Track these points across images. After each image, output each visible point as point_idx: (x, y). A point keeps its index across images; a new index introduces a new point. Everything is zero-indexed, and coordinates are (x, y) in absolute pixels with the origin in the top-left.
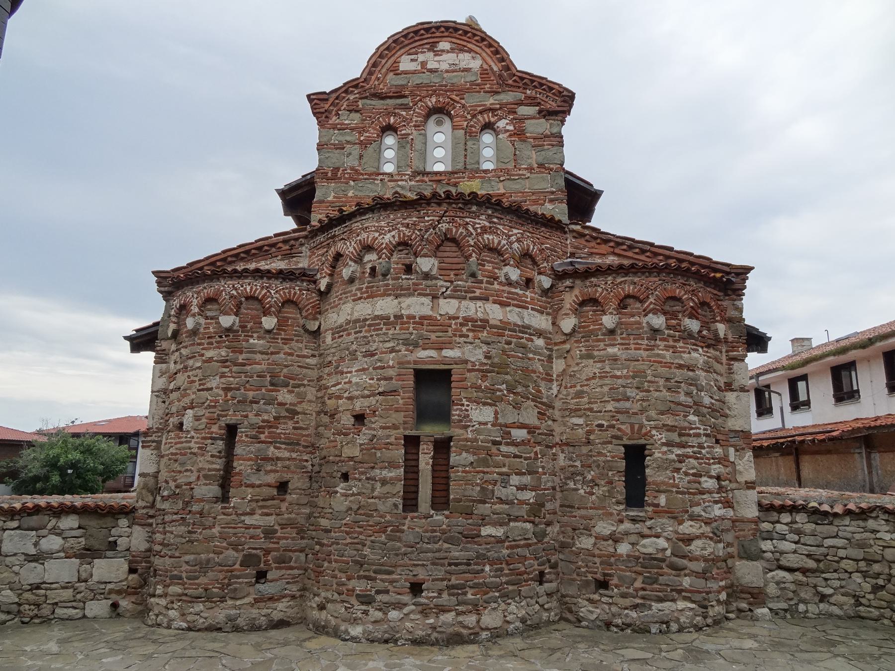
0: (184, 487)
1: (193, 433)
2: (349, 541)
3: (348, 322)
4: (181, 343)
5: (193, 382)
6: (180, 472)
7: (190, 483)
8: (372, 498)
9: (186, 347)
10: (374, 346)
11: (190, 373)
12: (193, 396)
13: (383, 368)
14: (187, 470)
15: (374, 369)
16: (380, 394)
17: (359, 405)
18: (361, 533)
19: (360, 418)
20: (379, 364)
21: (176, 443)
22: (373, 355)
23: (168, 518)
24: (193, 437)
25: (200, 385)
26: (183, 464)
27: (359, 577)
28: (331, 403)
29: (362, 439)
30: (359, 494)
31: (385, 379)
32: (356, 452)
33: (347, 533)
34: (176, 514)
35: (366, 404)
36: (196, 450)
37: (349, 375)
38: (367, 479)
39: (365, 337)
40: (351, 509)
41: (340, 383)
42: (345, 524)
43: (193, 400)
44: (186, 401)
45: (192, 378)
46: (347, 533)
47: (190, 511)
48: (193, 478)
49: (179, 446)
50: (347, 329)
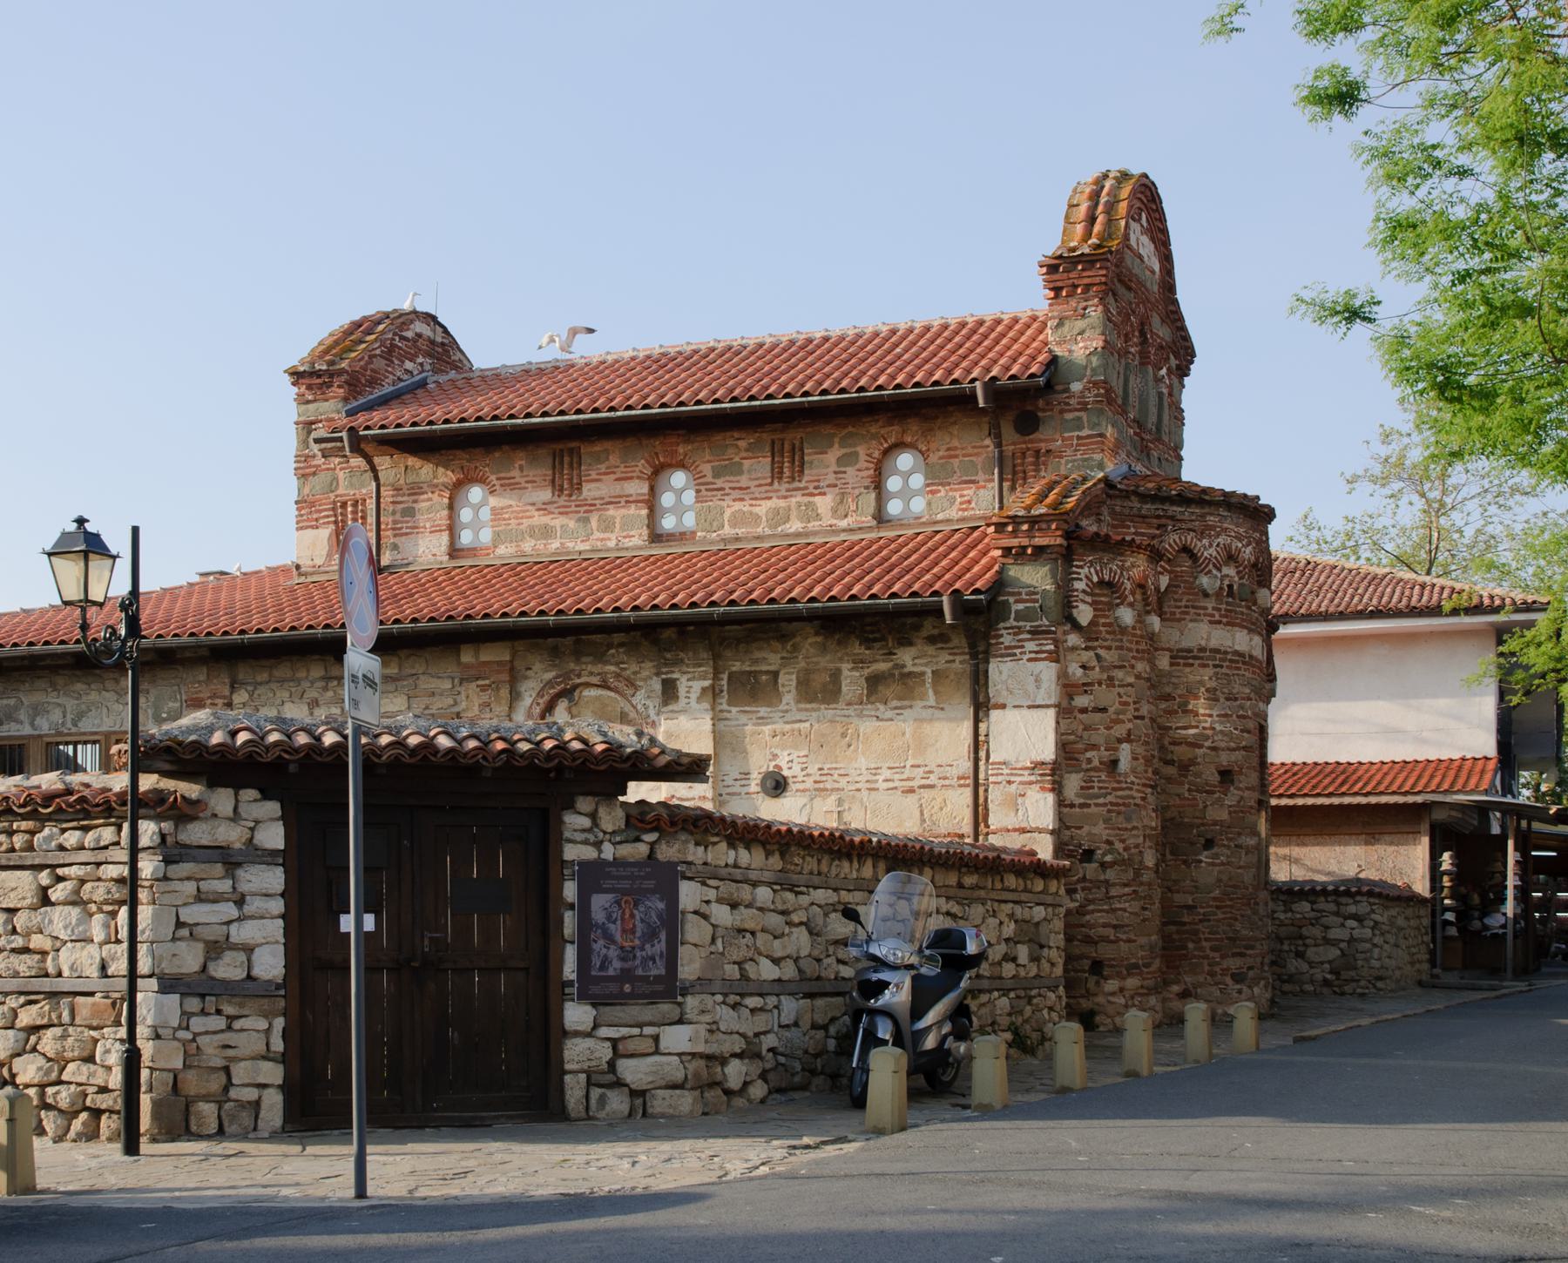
0: (1133, 851)
1: (1132, 778)
2: (1221, 916)
3: (1202, 650)
4: (1097, 639)
5: (1126, 704)
6: (1126, 829)
7: (1137, 846)
8: (1240, 867)
9: (1109, 648)
10: (1237, 688)
11: (1122, 690)
12: (1130, 726)
13: (1244, 717)
14: (1134, 828)
15: (1238, 717)
16: (1244, 748)
17: (1225, 759)
18: (1231, 907)
19: (1226, 775)
20: (1241, 712)
21: (1115, 789)
22: (1236, 699)
23: (1113, 892)
24: (1133, 783)
25: (1137, 710)
26: (1128, 819)
27: (1234, 955)
28: (1181, 752)
29: (1230, 800)
30: (1228, 863)
31: (1249, 732)
32: (1224, 815)
33: (1217, 907)
34: (1126, 885)
35: (1233, 758)
36: (1138, 801)
37: (1209, 719)
38: (1236, 846)
39: (1227, 675)
40: (1220, 880)
41: (1197, 727)
42: (1215, 899)
43: (1129, 730)
44: (1119, 731)
45: (1125, 699)
46: (1217, 907)
47: (1142, 884)
48: (1141, 840)
49: (1120, 793)
50: (1202, 658)
